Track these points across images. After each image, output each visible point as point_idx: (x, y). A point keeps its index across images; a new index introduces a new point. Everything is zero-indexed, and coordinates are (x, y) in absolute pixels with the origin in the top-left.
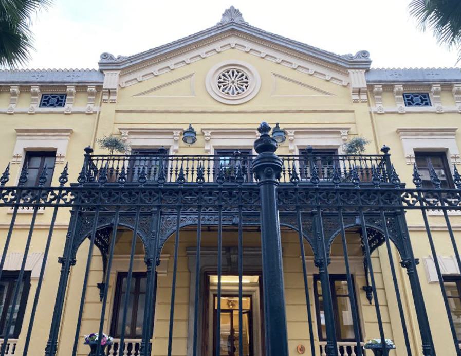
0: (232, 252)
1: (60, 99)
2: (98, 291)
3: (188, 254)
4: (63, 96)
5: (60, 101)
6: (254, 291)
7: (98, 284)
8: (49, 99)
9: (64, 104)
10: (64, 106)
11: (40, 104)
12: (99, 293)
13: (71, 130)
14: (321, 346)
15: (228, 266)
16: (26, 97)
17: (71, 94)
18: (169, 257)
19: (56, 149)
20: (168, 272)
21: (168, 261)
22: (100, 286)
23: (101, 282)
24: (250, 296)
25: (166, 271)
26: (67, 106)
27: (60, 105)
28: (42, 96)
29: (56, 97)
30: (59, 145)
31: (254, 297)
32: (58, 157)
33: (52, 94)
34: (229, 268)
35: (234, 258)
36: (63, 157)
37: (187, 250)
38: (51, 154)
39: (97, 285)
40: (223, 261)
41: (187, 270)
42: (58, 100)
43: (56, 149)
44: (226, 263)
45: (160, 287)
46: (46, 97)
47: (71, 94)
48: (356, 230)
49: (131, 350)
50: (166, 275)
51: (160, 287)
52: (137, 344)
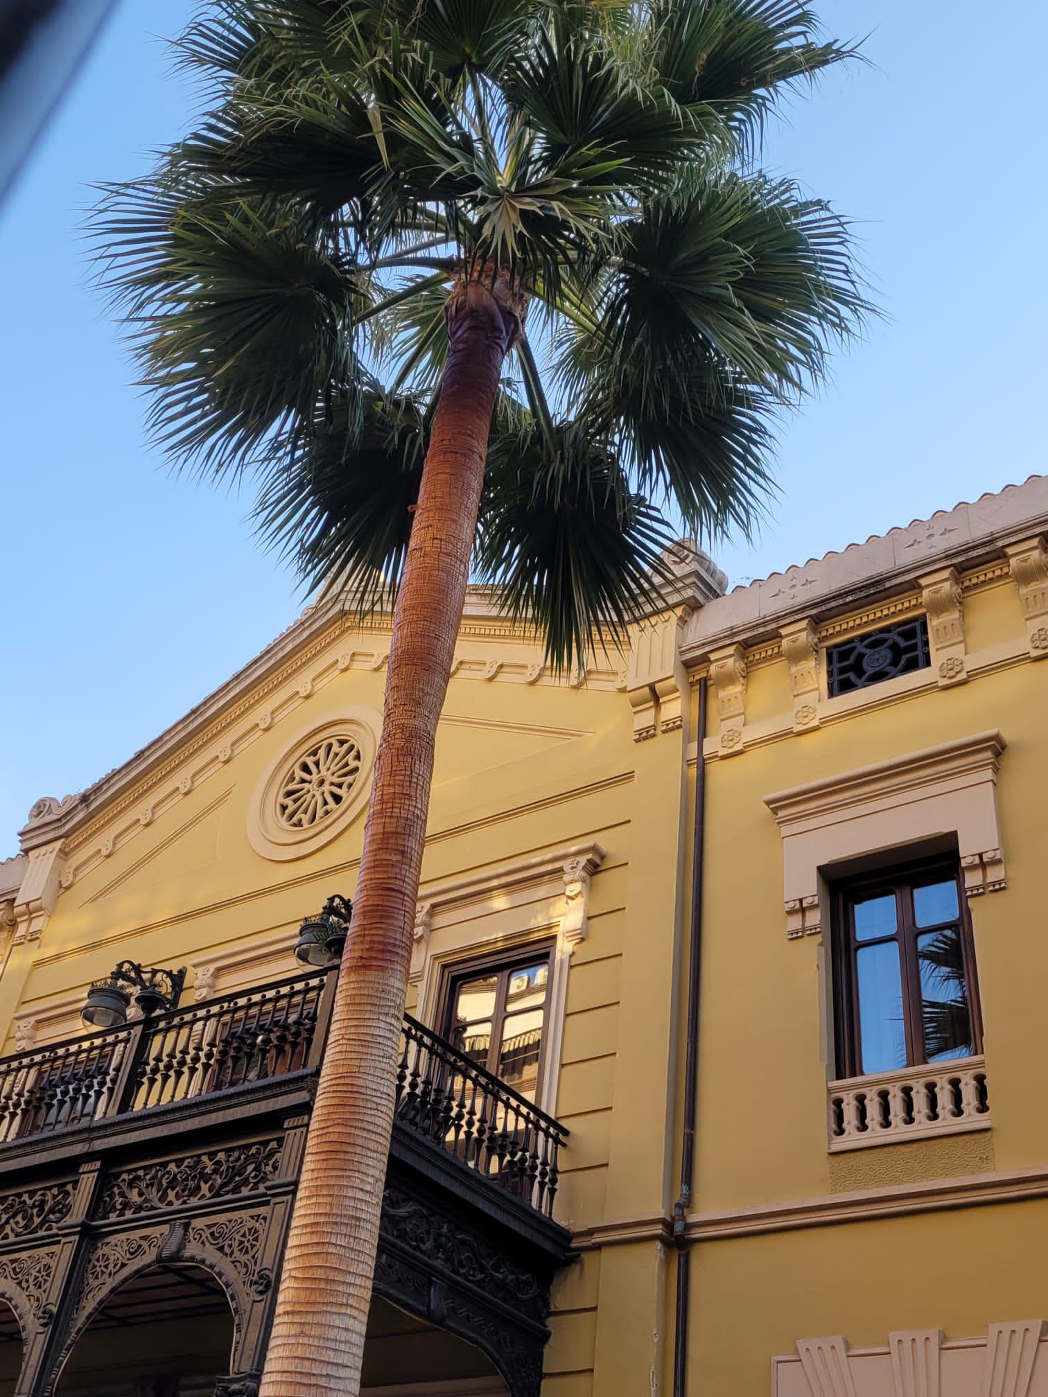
1: (903, 643)
4: (914, 629)
5: (905, 649)
8: (861, 656)
9: (927, 655)
10: (928, 664)
11: (830, 685)
13: (997, 738)
16: (770, 677)
17: (939, 607)
19: (954, 835)
26: (937, 657)
27: (912, 666)
28: (829, 656)
29: (885, 641)
30: (961, 812)
32: (972, 867)
33: (863, 638)
36: (995, 862)
38: (935, 860)
42: (897, 651)
43: (954, 835)
46: (844, 655)
47: (939, 607)
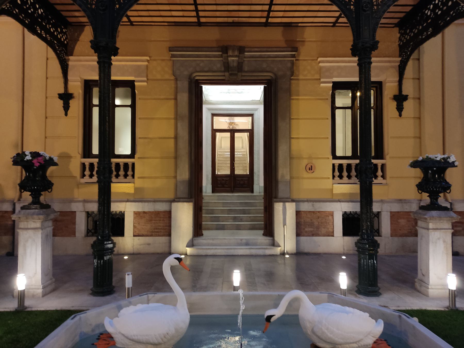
0: (230, 53)
2: (61, 102)
3: (173, 56)
6: (256, 110)
7: (59, 94)
12: (63, 105)
14: (334, 165)
15: (224, 72)
18: (148, 61)
20: (148, 79)
21: (147, 66)
22: (61, 96)
23: (62, 91)
24: (252, 115)
25: (145, 79)
31: (255, 117)
34: (227, 74)
35: (233, 60)
37: (170, 51)
39: (58, 96)
40: (217, 63)
41: (173, 78)
44: (223, 69)
45: (139, 99)
48: (396, 21)
49: (93, 171)
50: (146, 83)
51: (139, 99)
52: (92, 165)
